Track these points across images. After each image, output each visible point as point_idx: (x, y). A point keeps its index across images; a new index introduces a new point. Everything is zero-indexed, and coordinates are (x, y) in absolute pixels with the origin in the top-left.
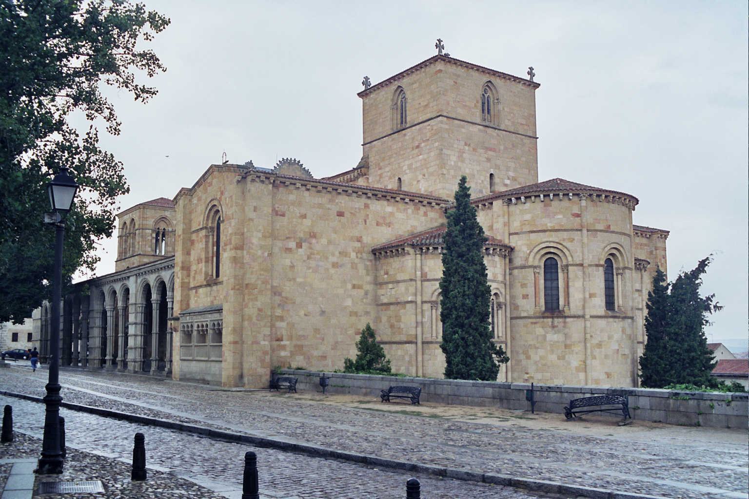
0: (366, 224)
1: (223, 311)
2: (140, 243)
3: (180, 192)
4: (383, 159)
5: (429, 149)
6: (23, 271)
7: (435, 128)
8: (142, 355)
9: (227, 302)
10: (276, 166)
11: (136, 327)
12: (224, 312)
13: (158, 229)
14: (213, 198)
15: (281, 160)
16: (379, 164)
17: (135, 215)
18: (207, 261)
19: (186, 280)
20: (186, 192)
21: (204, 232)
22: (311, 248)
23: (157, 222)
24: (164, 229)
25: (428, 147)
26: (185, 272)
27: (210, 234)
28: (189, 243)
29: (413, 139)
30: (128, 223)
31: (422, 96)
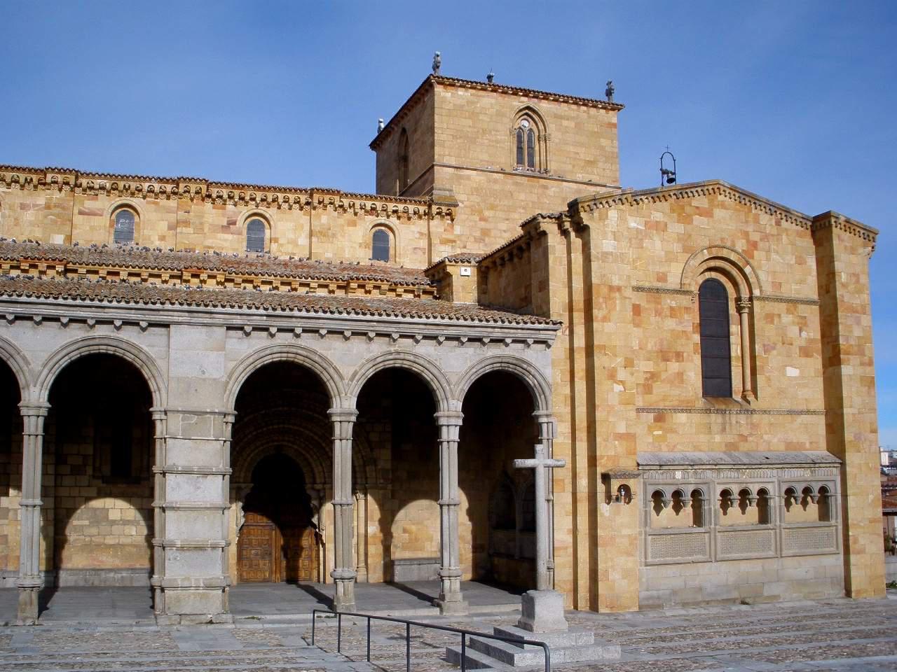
4: (492, 207)
14: (718, 243)
16: (480, 212)
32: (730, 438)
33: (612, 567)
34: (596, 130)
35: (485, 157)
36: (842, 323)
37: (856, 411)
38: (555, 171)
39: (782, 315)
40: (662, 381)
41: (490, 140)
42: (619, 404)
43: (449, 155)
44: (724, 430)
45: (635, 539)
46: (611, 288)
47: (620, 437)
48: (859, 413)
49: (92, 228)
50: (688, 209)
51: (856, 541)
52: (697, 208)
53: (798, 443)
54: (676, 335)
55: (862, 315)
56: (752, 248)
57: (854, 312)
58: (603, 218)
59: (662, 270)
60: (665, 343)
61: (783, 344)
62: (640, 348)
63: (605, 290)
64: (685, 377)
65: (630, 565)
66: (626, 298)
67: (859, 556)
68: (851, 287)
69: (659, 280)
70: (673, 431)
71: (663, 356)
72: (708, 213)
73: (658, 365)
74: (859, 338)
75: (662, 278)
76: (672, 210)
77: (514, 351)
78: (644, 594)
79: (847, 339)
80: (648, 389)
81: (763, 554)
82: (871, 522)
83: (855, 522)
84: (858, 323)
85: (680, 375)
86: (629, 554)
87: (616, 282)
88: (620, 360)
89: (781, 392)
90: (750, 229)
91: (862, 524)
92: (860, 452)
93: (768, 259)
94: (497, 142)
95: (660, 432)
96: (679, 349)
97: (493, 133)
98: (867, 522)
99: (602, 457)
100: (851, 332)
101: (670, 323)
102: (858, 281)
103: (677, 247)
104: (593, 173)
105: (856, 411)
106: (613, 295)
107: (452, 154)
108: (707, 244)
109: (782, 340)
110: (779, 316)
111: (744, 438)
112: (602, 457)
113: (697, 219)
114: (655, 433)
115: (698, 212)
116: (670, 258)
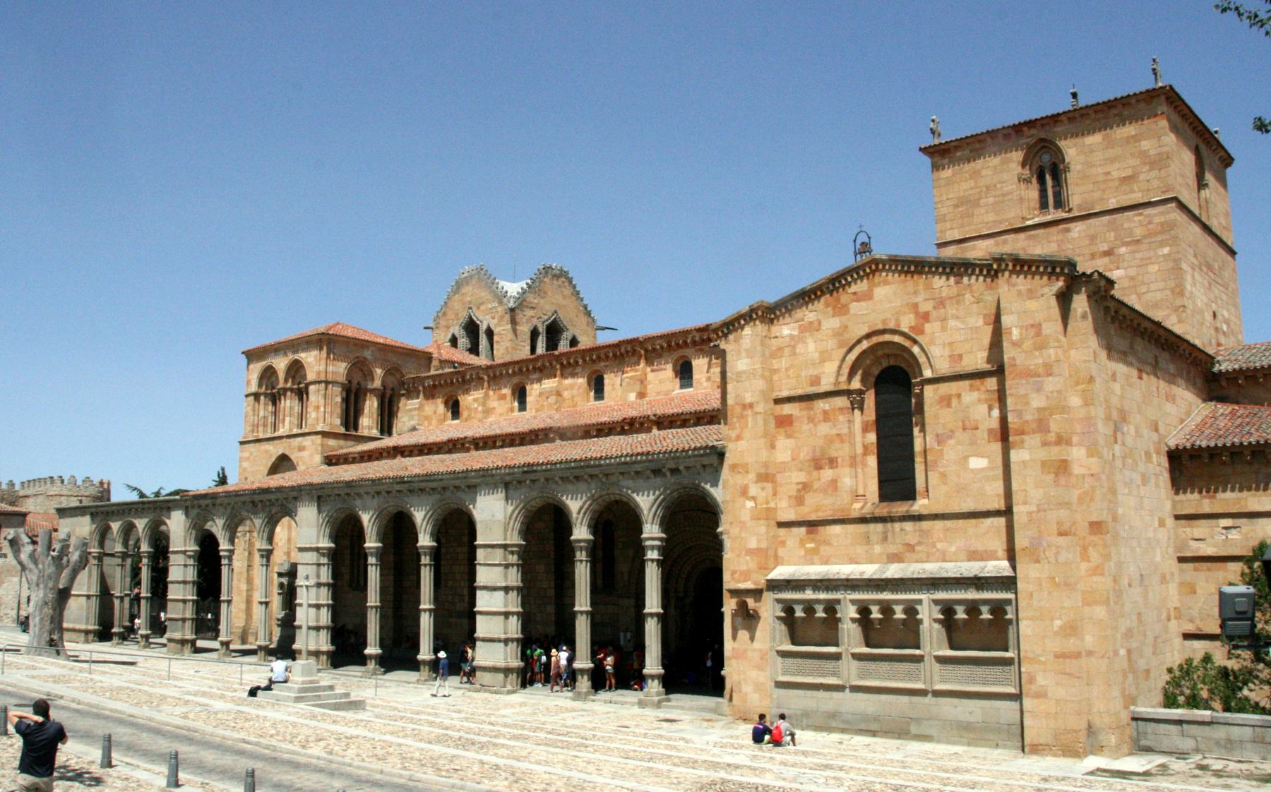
5: (1142, 259)
7: (1157, 220)
9: (1038, 561)
14: (880, 327)
19: (772, 505)
21: (842, 402)
22: (1123, 444)
25: (1138, 255)
26: (769, 486)
28: (772, 424)
29: (1093, 238)
31: (1112, 160)
32: (893, 549)
33: (745, 679)
34: (1133, 133)
35: (991, 217)
36: (1011, 395)
37: (1035, 509)
38: (1079, 206)
39: (963, 394)
40: (815, 491)
41: (995, 196)
43: (952, 229)
44: (885, 539)
46: (744, 407)
47: (750, 552)
48: (1039, 511)
49: (661, 382)
51: (1032, 680)
52: (855, 293)
53: (986, 551)
54: (829, 440)
55: (1046, 379)
56: (922, 321)
57: (1032, 376)
59: (815, 372)
61: (964, 429)
63: (738, 410)
64: (839, 484)
65: (762, 679)
66: (757, 413)
67: (1036, 701)
68: (1027, 344)
69: (812, 385)
70: (826, 543)
71: (816, 464)
72: (868, 296)
74: (1040, 410)
75: (816, 381)
76: (827, 305)
79: (1019, 414)
80: (799, 500)
82: (1057, 656)
83: (1031, 655)
85: (834, 483)
86: (760, 668)
87: (748, 398)
88: (752, 476)
89: (961, 489)
90: (919, 299)
91: (1042, 659)
93: (944, 329)
94: (1004, 195)
95: (812, 545)
96: (833, 454)
97: (999, 186)
98: (1052, 658)
100: (1027, 403)
101: (824, 429)
102: (1038, 334)
103: (831, 344)
104: (1133, 191)
105: (1035, 509)
106: (746, 413)
107: (955, 226)
108: (865, 330)
110: (959, 396)
113: (854, 307)
114: (808, 546)
115: (852, 297)
116: (824, 357)
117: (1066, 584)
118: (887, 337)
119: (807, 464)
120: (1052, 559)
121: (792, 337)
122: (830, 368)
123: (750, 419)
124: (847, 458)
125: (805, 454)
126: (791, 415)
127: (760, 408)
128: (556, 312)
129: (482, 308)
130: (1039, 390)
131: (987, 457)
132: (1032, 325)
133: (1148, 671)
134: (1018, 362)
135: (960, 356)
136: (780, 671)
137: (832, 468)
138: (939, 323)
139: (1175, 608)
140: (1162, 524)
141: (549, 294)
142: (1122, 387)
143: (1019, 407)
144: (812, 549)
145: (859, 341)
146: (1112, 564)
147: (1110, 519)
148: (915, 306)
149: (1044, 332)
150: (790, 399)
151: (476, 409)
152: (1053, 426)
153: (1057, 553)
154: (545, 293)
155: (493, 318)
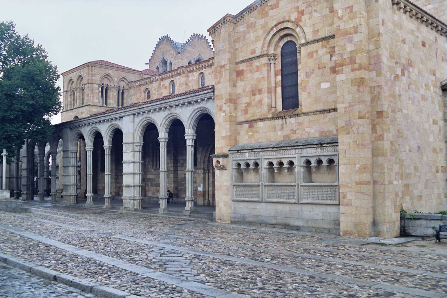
0: (437, 58)
1: (339, 144)
2: (90, 96)
3: (224, 18)
6: (12, 110)
8: (141, 193)
10: (189, 39)
11: (134, 166)
12: (340, 147)
13: (103, 84)
14: (282, 20)
15: (193, 35)
17: (84, 73)
18: (269, 92)
19: (234, 114)
20: (231, 19)
21: (264, 60)
22: (409, 77)
23: (102, 79)
24: (107, 85)
27: (272, 62)
28: (235, 75)
30: (75, 79)
32: (286, 133)
40: (253, 106)
42: (224, 122)
44: (282, 128)
45: (229, 187)
48: (350, 106)
50: (266, 9)
51: (344, 197)
52: (271, 5)
54: (259, 80)
55: (355, 35)
57: (348, 34)
58: (220, 33)
60: (254, 85)
61: (319, 68)
62: (243, 92)
64: (263, 102)
67: (346, 208)
70: (257, 132)
73: (251, 98)
74: (351, 52)
75: (253, 52)
77: (202, 105)
78: (233, 215)
80: (246, 112)
81: (290, 201)
82: (357, 184)
83: (345, 184)
84: (351, 41)
85: (261, 101)
87: (223, 63)
88: (224, 101)
91: (350, 185)
92: (349, 134)
93: (311, 18)
95: (251, 133)
96: (260, 87)
98: (355, 184)
99: (217, 149)
100: (345, 49)
101: (257, 75)
102: (351, 11)
105: (347, 105)
106: (222, 70)
108: (275, 23)
109: (319, 66)
110: (317, 51)
111: (294, 131)
112: (217, 147)
113: (271, 13)
114: (249, 134)
115: (270, 7)
116: (257, 40)
117: (362, 145)
118: (285, 25)
119: (249, 93)
120: (356, 132)
121: (244, 31)
122: (259, 45)
123: (223, 73)
124: (267, 88)
125: (248, 89)
126: (243, 70)
127: (227, 67)
128: (200, 54)
129: (168, 53)
130: (351, 41)
131: (329, 82)
132: (348, 7)
133: (421, 197)
134: (341, 28)
135: (318, 30)
136: (235, 195)
137: (259, 94)
138: (308, 15)
139: (442, 167)
140: (435, 122)
141: (197, 46)
142: (409, 47)
143: (341, 52)
144: (251, 135)
145: (272, 29)
146: (390, 135)
147: (390, 110)
148: (298, 7)
149: (354, 10)
150: (242, 62)
151: (155, 93)
152: (357, 61)
153: (358, 128)
154: (195, 46)
155: (172, 57)
